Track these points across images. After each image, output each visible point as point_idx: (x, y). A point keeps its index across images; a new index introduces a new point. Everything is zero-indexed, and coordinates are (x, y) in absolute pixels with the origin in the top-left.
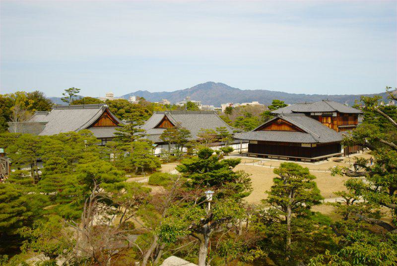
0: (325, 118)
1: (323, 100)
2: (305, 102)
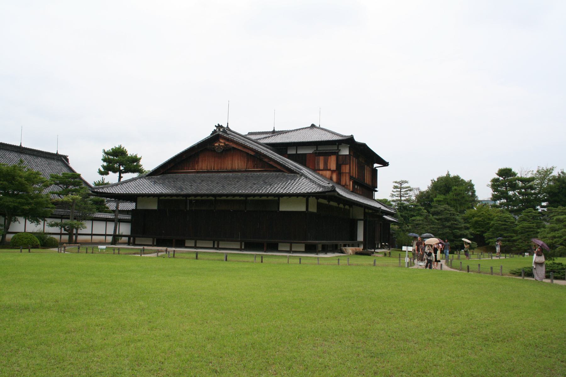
0: (322, 159)
1: (313, 126)
2: (272, 130)
